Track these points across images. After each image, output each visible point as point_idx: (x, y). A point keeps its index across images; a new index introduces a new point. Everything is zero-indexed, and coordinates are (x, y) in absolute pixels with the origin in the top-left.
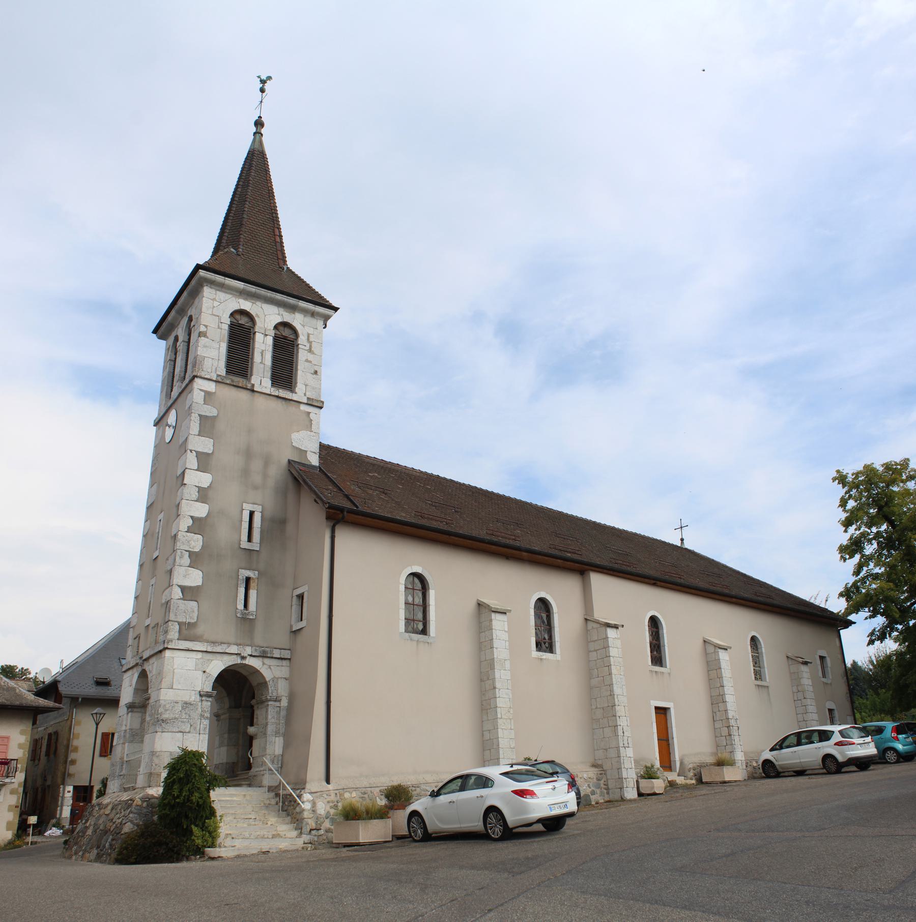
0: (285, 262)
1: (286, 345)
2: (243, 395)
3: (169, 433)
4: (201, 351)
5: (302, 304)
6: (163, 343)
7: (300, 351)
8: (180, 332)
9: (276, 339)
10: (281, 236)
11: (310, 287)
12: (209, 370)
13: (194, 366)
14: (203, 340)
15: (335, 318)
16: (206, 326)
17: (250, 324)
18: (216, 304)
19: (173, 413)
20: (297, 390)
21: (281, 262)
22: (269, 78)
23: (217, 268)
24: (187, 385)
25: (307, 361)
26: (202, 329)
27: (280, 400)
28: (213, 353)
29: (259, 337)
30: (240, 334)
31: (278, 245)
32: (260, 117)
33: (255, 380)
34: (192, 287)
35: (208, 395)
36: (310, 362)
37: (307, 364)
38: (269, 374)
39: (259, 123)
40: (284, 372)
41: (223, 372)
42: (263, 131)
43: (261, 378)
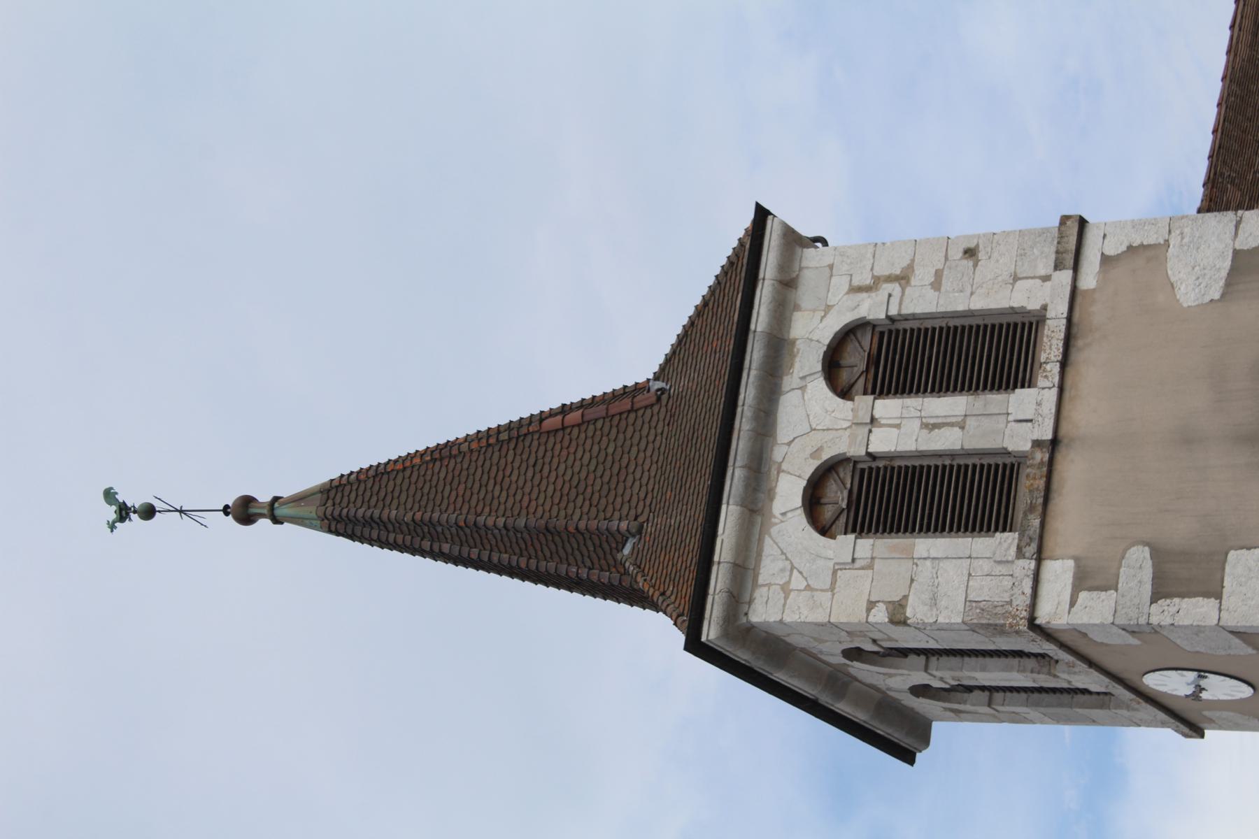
0: (638, 389)
1: (896, 357)
2: (1074, 471)
3: (1220, 689)
4: (951, 613)
5: (761, 319)
6: (938, 729)
7: (906, 311)
8: (898, 681)
9: (881, 389)
10: (565, 409)
11: (705, 302)
12: (1007, 582)
13: (999, 630)
14: (916, 611)
15: (791, 212)
16: (871, 605)
17: (846, 473)
18: (797, 582)
19: (1156, 682)
20: (1033, 305)
21: (641, 400)
22: (109, 495)
23: (688, 590)
24: (1063, 646)
25: (936, 285)
26: (880, 615)
27: (1075, 356)
28: (952, 579)
29: (883, 442)
30: (880, 498)
31: (591, 413)
32: (226, 510)
33: (1018, 440)
34: (759, 660)
35: (1084, 580)
36: (939, 274)
37: (946, 284)
38: (994, 400)
39: (244, 511)
40: (988, 352)
41: (1006, 541)
42: (264, 497)
43: (1005, 421)
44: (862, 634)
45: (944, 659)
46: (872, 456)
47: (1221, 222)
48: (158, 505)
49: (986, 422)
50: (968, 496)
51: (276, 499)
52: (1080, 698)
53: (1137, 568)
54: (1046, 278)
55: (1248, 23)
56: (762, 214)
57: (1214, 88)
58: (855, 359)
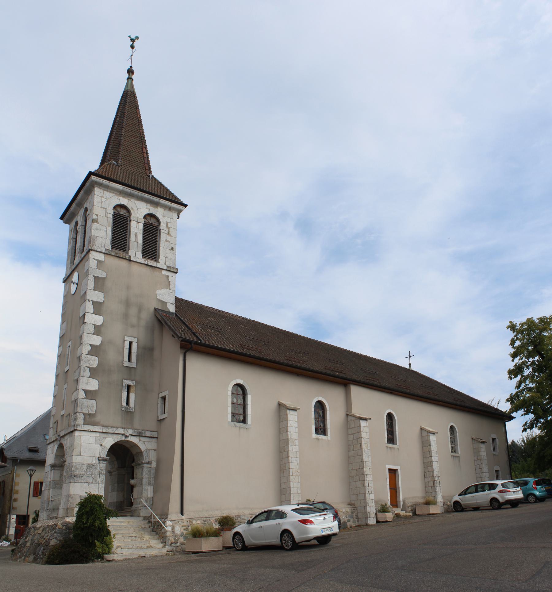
0: (150, 171)
1: (152, 229)
2: (124, 263)
3: (73, 288)
4: (94, 233)
5: (163, 201)
6: (68, 226)
7: (161, 233)
8: (79, 218)
9: (145, 225)
10: (147, 154)
11: (168, 190)
12: (100, 246)
13: (90, 242)
14: (95, 224)
15: (185, 212)
16: (97, 215)
17: (127, 215)
18: (103, 200)
19: (76, 275)
20: (160, 260)
21: (148, 172)
22: (137, 38)
23: (104, 174)
24: (85, 256)
25: (166, 241)
26: (95, 217)
27: (148, 267)
28: (103, 234)
29: (133, 224)
30: (121, 221)
31: (146, 159)
32: (131, 67)
33: (131, 253)
34: (86, 188)
35: (99, 262)
36: (169, 241)
37: (166, 243)
38: (140, 249)
39: (130, 71)
40: (151, 248)
41: (109, 247)
42: (133, 77)
43: (135, 250)
44: (91, 212)
45: (84, 230)
46: (130, 221)
47: (173, 300)
48: (134, 50)
49: (136, 247)
50: (120, 240)
51: (133, 80)
52: (73, 258)
53: (101, 274)
54: (165, 264)
55: (212, 311)
56: (186, 206)
57: (200, 302)
58: (152, 221)
